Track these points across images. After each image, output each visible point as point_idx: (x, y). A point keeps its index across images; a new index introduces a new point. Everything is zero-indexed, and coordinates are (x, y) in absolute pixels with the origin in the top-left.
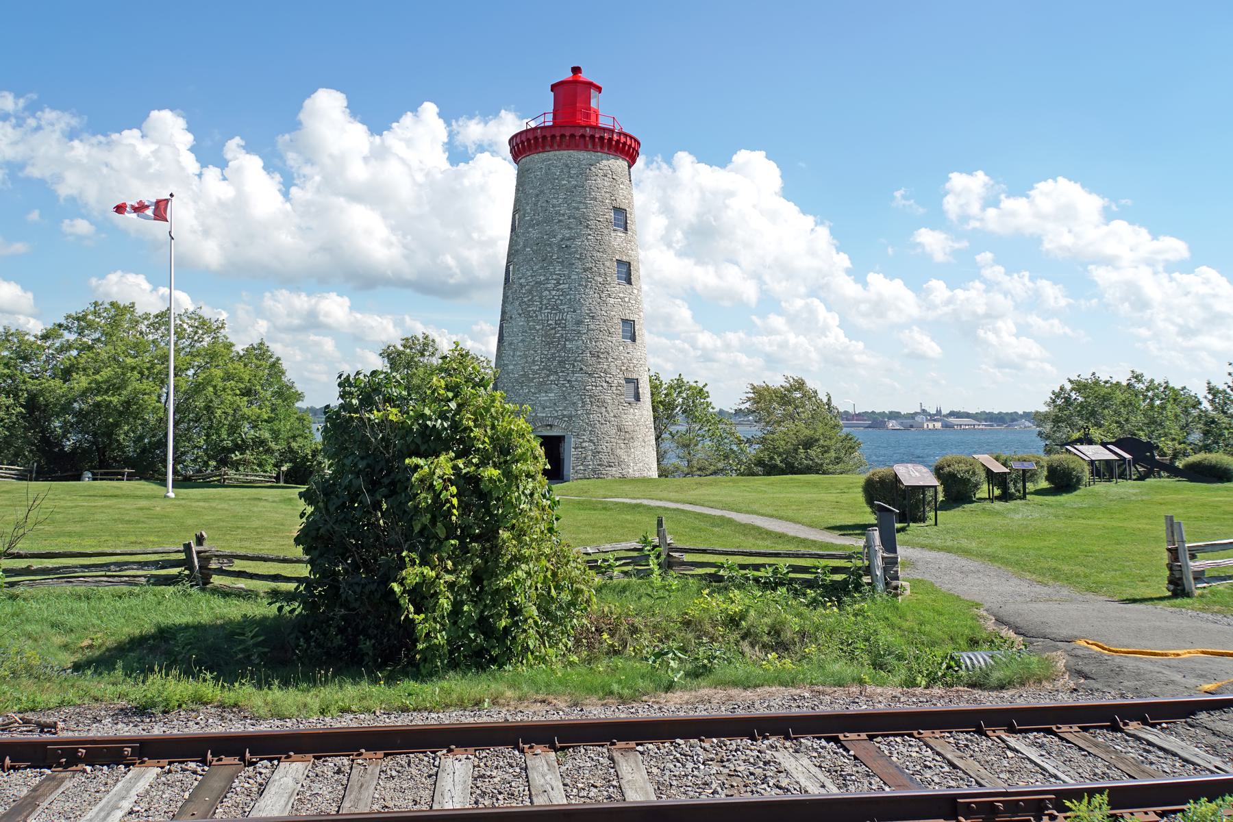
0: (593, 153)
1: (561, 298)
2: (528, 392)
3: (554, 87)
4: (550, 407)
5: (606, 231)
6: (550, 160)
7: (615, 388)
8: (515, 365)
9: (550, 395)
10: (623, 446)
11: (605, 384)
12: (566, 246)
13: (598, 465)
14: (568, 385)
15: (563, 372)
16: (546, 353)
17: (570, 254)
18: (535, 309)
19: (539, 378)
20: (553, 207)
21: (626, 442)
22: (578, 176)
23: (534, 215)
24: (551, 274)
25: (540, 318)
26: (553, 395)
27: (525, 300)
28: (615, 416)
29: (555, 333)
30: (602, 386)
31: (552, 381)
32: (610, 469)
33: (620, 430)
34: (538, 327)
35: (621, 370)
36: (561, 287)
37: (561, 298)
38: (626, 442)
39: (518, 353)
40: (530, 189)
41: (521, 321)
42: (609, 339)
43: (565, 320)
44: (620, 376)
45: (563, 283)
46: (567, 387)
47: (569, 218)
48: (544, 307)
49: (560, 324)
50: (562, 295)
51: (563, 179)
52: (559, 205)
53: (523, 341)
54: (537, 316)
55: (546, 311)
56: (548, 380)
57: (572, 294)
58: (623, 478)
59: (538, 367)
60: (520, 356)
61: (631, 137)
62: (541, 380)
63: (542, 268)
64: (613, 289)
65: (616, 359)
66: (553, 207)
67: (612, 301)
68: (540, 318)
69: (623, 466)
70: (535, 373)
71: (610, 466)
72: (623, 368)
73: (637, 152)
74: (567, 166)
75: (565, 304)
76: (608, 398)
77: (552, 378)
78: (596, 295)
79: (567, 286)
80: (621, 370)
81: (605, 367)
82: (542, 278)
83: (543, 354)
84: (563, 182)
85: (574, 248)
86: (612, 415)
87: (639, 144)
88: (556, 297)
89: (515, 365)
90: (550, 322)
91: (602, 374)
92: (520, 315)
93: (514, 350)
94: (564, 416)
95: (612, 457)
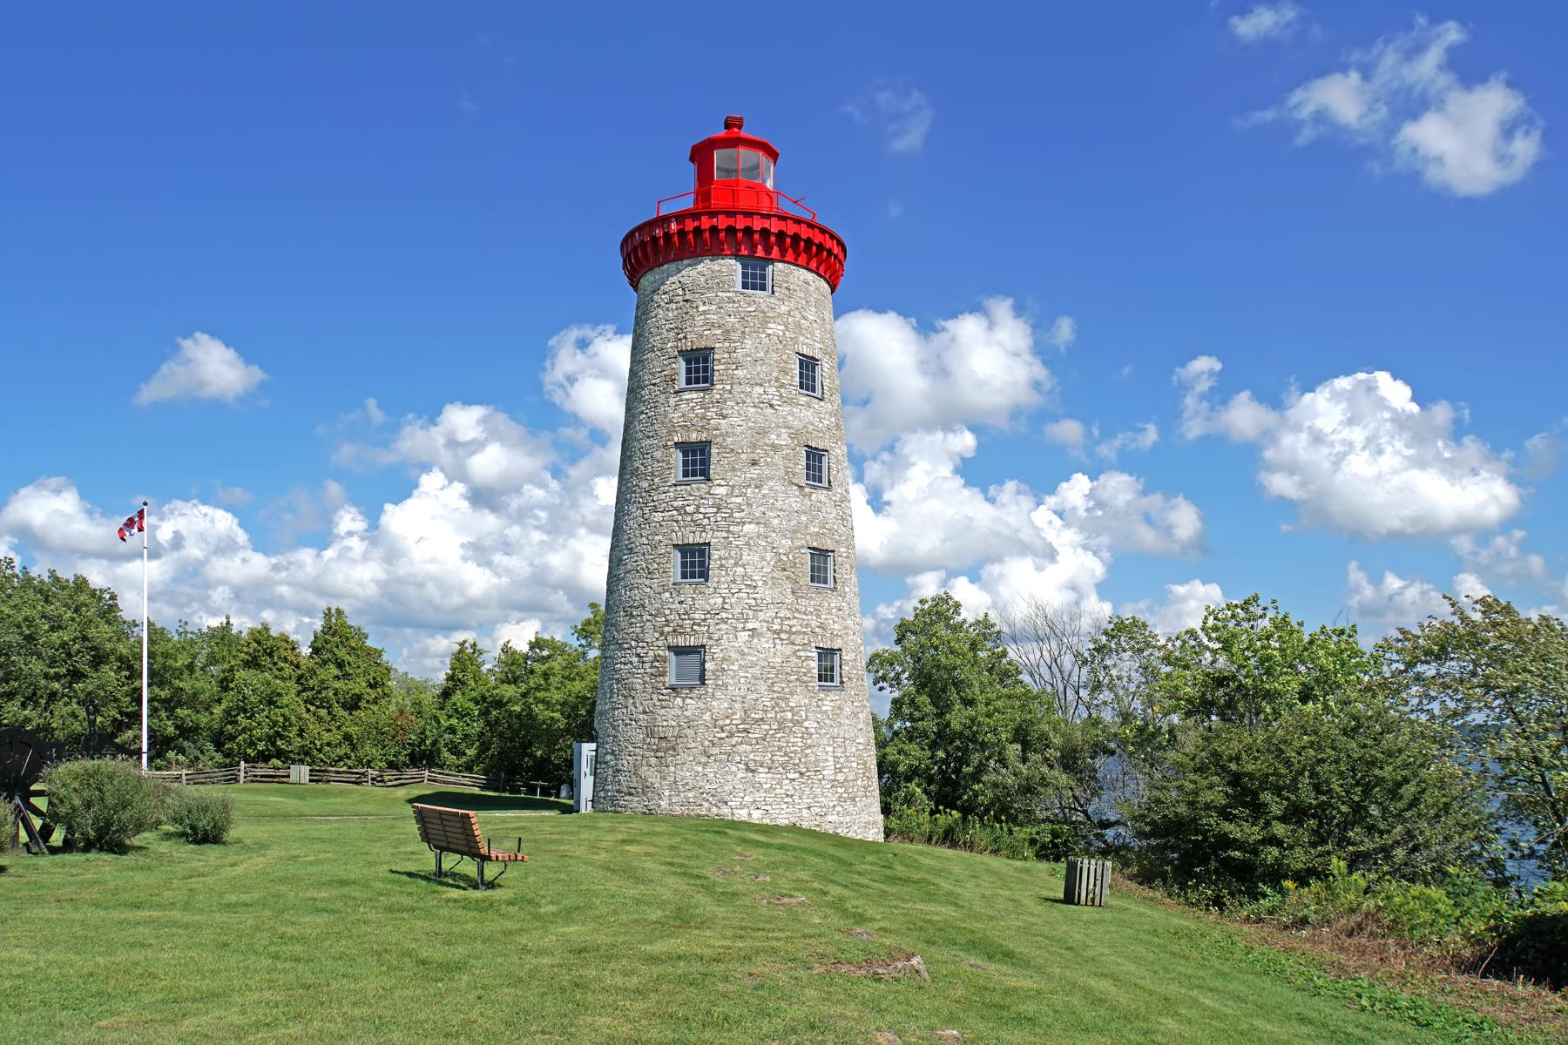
10: (653, 761)
11: (635, 659)
21: (659, 754)
28: (645, 712)
30: (631, 663)
35: (662, 634)
38: (659, 754)
44: (660, 643)
58: (649, 813)
65: (656, 616)
67: (658, 517)
69: (650, 794)
71: (631, 794)
72: (666, 629)
76: (637, 682)
80: (662, 634)
81: (638, 630)
86: (641, 709)
95: (634, 779)
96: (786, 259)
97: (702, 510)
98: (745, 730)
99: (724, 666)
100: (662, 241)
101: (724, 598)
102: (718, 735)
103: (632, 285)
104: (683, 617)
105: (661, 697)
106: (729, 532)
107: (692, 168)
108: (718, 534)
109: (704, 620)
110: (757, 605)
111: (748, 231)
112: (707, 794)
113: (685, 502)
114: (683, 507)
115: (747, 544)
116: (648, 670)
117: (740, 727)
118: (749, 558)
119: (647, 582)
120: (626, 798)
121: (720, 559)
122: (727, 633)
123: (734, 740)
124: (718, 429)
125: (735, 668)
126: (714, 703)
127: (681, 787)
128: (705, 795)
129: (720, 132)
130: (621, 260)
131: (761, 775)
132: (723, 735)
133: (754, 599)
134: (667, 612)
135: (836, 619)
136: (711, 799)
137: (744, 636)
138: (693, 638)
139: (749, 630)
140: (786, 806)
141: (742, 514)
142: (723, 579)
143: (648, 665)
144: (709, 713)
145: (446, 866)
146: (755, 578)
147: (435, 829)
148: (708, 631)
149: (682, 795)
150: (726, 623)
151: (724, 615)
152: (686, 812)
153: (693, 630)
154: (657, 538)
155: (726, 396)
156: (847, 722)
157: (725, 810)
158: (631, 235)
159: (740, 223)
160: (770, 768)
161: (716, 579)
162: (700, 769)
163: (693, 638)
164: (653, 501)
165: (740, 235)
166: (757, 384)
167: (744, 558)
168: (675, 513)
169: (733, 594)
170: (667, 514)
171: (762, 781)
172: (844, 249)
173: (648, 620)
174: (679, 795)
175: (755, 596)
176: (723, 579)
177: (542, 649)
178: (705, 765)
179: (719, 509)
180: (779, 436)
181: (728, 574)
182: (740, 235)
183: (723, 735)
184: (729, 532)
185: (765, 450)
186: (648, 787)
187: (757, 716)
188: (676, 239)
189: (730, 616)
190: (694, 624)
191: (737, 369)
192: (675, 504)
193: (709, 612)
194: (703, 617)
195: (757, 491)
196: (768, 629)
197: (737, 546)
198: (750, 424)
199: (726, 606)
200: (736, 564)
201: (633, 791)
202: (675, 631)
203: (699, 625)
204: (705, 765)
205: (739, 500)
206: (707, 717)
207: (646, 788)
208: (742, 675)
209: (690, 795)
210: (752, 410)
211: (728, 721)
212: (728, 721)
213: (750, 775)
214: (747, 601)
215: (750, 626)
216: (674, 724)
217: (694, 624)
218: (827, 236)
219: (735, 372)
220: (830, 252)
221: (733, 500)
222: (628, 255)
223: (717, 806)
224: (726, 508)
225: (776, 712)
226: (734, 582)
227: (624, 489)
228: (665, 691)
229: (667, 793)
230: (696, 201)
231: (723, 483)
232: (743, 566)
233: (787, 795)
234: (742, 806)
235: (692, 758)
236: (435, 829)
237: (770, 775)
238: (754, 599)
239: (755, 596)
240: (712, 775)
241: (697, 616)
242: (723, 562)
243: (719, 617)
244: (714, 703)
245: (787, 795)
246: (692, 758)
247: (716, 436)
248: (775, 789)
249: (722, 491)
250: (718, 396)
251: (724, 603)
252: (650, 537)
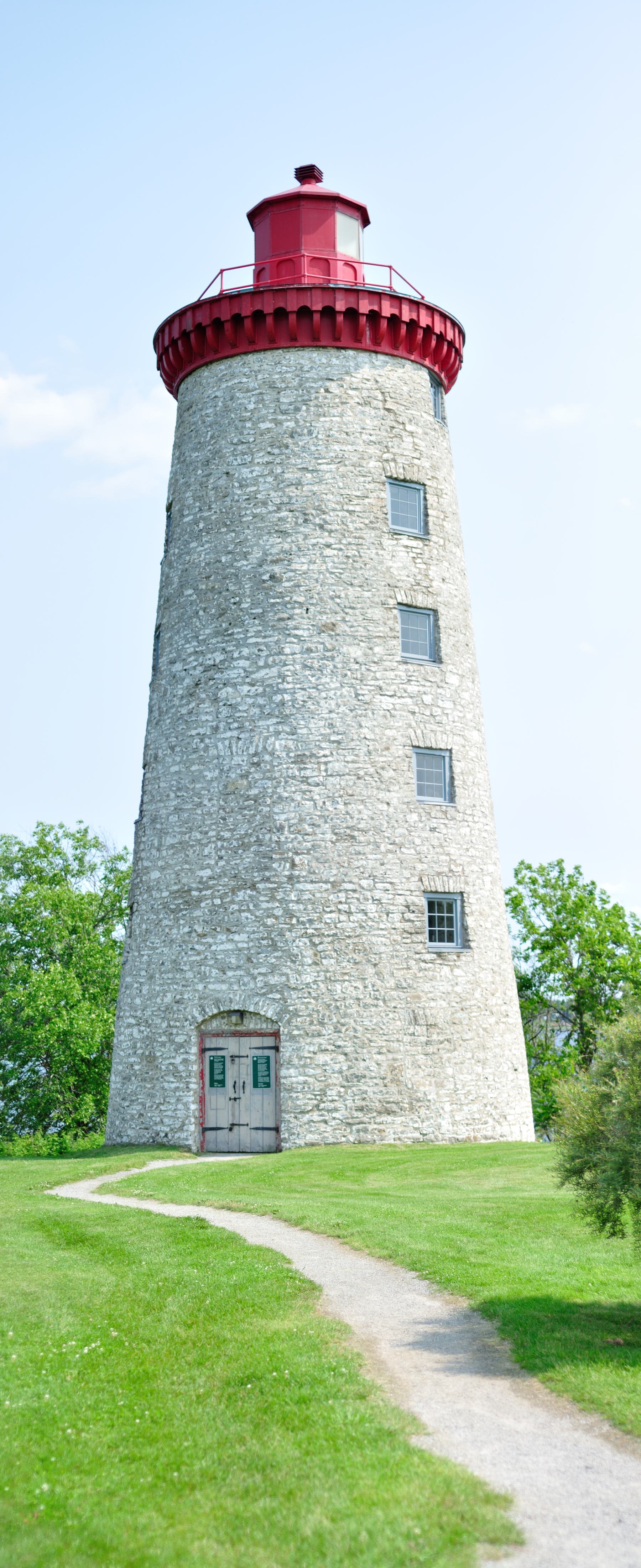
0: (333, 352)
1: (261, 701)
2: (190, 932)
3: (254, 216)
4: (238, 967)
5: (370, 536)
6: (233, 376)
7: (397, 917)
8: (162, 869)
9: (236, 937)
10: (421, 1058)
12: (272, 577)
13: (361, 1109)
14: (279, 912)
15: (267, 880)
16: (227, 835)
17: (281, 595)
18: (201, 731)
19: (213, 897)
20: (241, 486)
22: (297, 409)
23: (201, 510)
24: (238, 646)
25: (213, 752)
26: (243, 937)
27: (184, 711)
28: (398, 987)
29: (250, 787)
31: (241, 903)
32: (389, 1119)
33: (415, 1020)
34: (209, 775)
36: (262, 673)
37: (261, 701)
39: (169, 840)
40: (195, 450)
41: (175, 763)
42: (381, 795)
43: (272, 754)
45: (267, 666)
46: (276, 918)
47: (279, 509)
48: (222, 725)
49: (257, 764)
50: (263, 694)
51: (263, 419)
52: (255, 481)
53: (178, 810)
54: (206, 749)
55: (229, 734)
56: (232, 902)
57: (285, 691)
59: (207, 873)
60: (172, 846)
61: (444, 317)
62: (218, 901)
63: (217, 633)
64: (391, 674)
66: (241, 486)
68: (213, 752)
70: (204, 885)
71: (389, 1112)
73: (458, 353)
74: (272, 386)
75: (271, 716)
77: (241, 895)
78: (345, 691)
79: (274, 671)
82: (219, 657)
83: (221, 839)
84: (263, 426)
85: (288, 580)
86: (392, 983)
87: (461, 333)
88: (250, 701)
89: (162, 869)
90: (237, 760)
91: (364, 883)
92: (172, 748)
93: (163, 833)
94: (272, 988)
95: (393, 1088)
105: (423, 965)
113: (422, 689)
116: (398, 925)
120: (378, 1120)
126: (481, 975)
127: (463, 1098)
128: (489, 1108)
136: (494, 1112)
149: (465, 1108)
152: (472, 1134)
168: (409, 701)
174: (461, 1110)
186: (418, 1100)
201: (394, 1107)
204: (483, 1063)
207: (415, 1103)
209: (475, 1107)
228: (428, 957)
229: (448, 1107)
230: (258, 275)
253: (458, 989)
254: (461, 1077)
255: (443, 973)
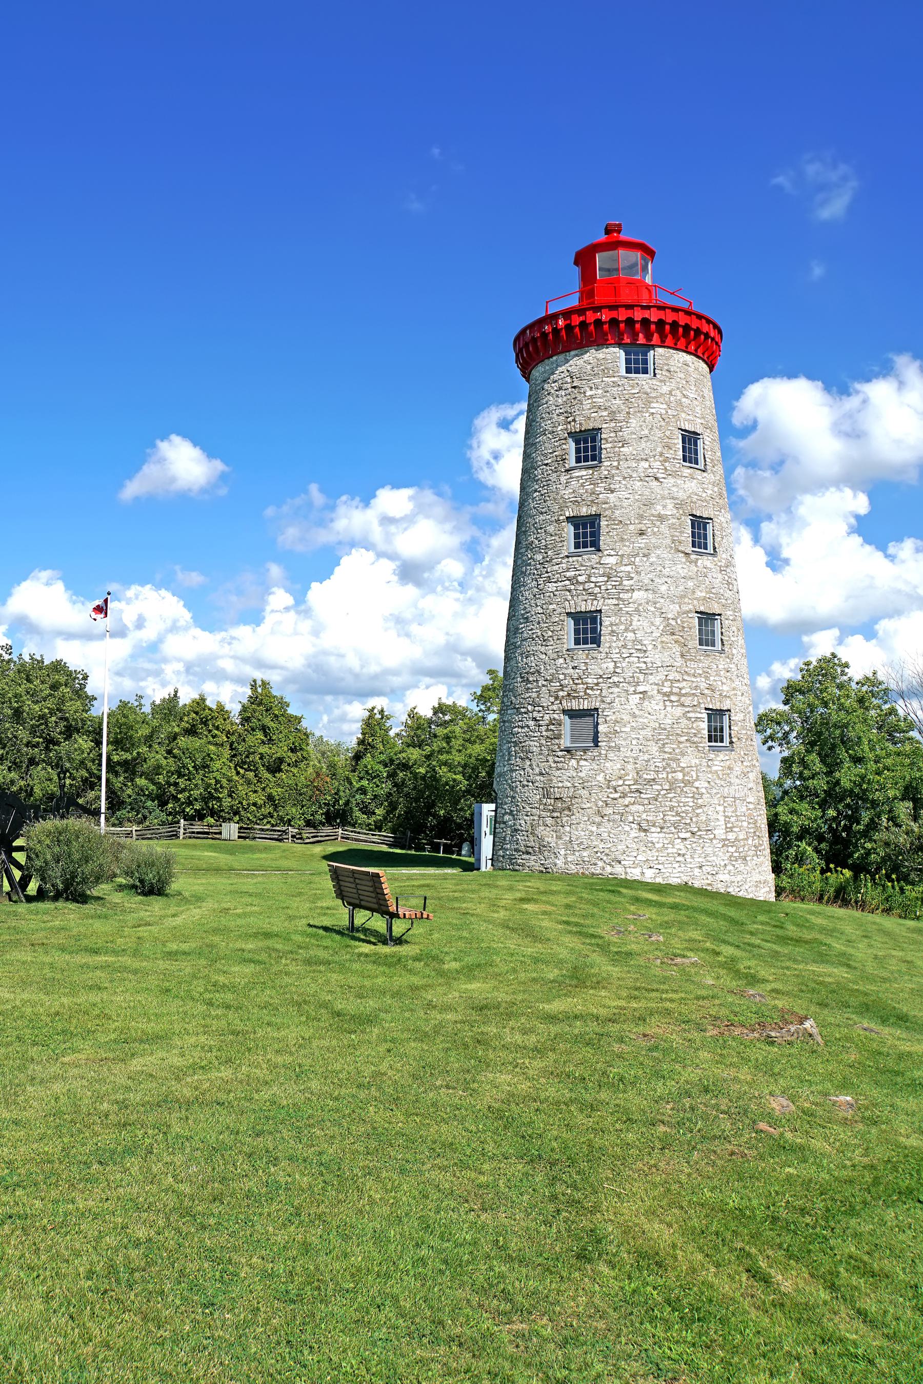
10: (549, 821)
11: (531, 723)
21: (555, 814)
28: (541, 774)
30: (528, 726)
32: (527, 857)
35: (557, 698)
38: (555, 814)
44: (555, 707)
58: (545, 872)
65: (551, 681)
67: (551, 587)
69: (546, 853)
71: (528, 853)
72: (561, 694)
76: (534, 745)
80: (557, 698)
81: (534, 695)
86: (537, 770)
95: (532, 839)
96: (666, 344)
97: (593, 579)
98: (638, 791)
99: (616, 728)
100: (550, 337)
101: (615, 662)
102: (612, 796)
103: (524, 376)
104: (576, 681)
105: (557, 759)
106: (619, 599)
107: (576, 270)
108: (610, 601)
109: (597, 684)
110: (647, 669)
111: (630, 322)
112: (601, 853)
113: (577, 573)
114: (575, 577)
115: (637, 610)
116: (544, 733)
117: (632, 787)
118: (639, 623)
119: (543, 649)
120: (523, 857)
121: (611, 625)
122: (618, 696)
123: (627, 801)
124: (606, 503)
125: (627, 729)
127: (576, 846)
128: (599, 854)
129: (602, 237)
130: (513, 355)
131: (653, 835)
132: (617, 795)
133: (645, 663)
134: (561, 677)
135: (724, 681)
136: (605, 858)
137: (635, 699)
138: (586, 702)
139: (640, 693)
140: (678, 864)
141: (631, 582)
142: (614, 645)
143: (543, 728)
144: (602, 774)
145: (358, 922)
146: (645, 642)
147: (348, 887)
148: (600, 695)
149: (577, 853)
150: (618, 687)
151: (616, 679)
152: (581, 871)
153: (586, 694)
154: (551, 607)
155: (613, 472)
156: (738, 781)
157: (618, 870)
158: (523, 332)
159: (622, 315)
160: (662, 828)
161: (607, 645)
162: (594, 829)
163: (586, 702)
164: (547, 572)
165: (622, 325)
166: (642, 459)
167: (634, 623)
168: (567, 582)
169: (624, 658)
170: (560, 584)
171: (655, 840)
172: (720, 332)
173: (543, 686)
174: (574, 854)
175: (645, 660)
176: (614, 645)
177: (444, 714)
178: (599, 825)
179: (609, 578)
180: (664, 507)
181: (618, 640)
182: (622, 325)
183: (617, 795)
184: (619, 599)
185: (652, 521)
186: (544, 846)
187: (649, 777)
188: (563, 333)
189: (622, 680)
190: (587, 688)
191: (623, 446)
192: (568, 574)
193: (601, 677)
194: (595, 681)
195: (645, 559)
196: (659, 692)
197: (627, 613)
198: (637, 497)
199: (618, 670)
200: (626, 630)
201: (530, 850)
202: (569, 695)
203: (592, 689)
204: (599, 825)
205: (628, 568)
206: (600, 778)
207: (543, 847)
208: (634, 736)
209: (585, 854)
210: (639, 484)
211: (621, 782)
212: (621, 782)
213: (643, 834)
214: (638, 665)
215: (641, 689)
216: (569, 785)
217: (587, 688)
218: (704, 321)
219: (622, 449)
220: (707, 335)
221: (623, 568)
222: (521, 351)
223: (610, 865)
224: (616, 576)
225: (668, 773)
226: (624, 646)
227: (519, 562)
228: (560, 754)
229: (563, 852)
231: (612, 553)
232: (634, 631)
233: (679, 854)
234: (635, 865)
235: (586, 819)
236: (348, 887)
237: (662, 835)
238: (645, 663)
239: (645, 660)
240: (606, 834)
241: (589, 681)
242: (614, 628)
243: (611, 681)
244: (607, 764)
245: (679, 854)
246: (586, 819)
247: (605, 509)
248: (667, 848)
249: (612, 560)
250: (606, 473)
251: (616, 667)
252: (544, 607)
253: (582, 775)
254: (576, 833)
255: (570, 764)
